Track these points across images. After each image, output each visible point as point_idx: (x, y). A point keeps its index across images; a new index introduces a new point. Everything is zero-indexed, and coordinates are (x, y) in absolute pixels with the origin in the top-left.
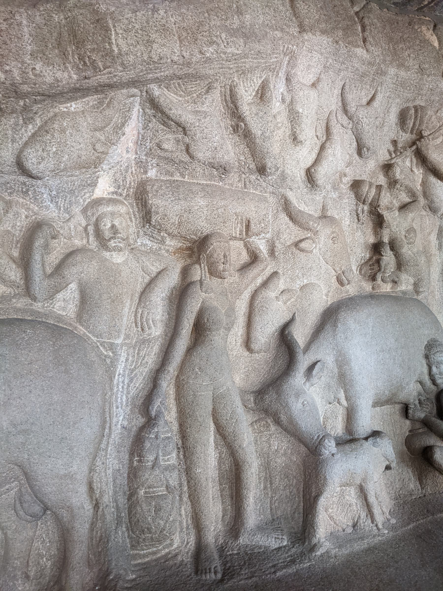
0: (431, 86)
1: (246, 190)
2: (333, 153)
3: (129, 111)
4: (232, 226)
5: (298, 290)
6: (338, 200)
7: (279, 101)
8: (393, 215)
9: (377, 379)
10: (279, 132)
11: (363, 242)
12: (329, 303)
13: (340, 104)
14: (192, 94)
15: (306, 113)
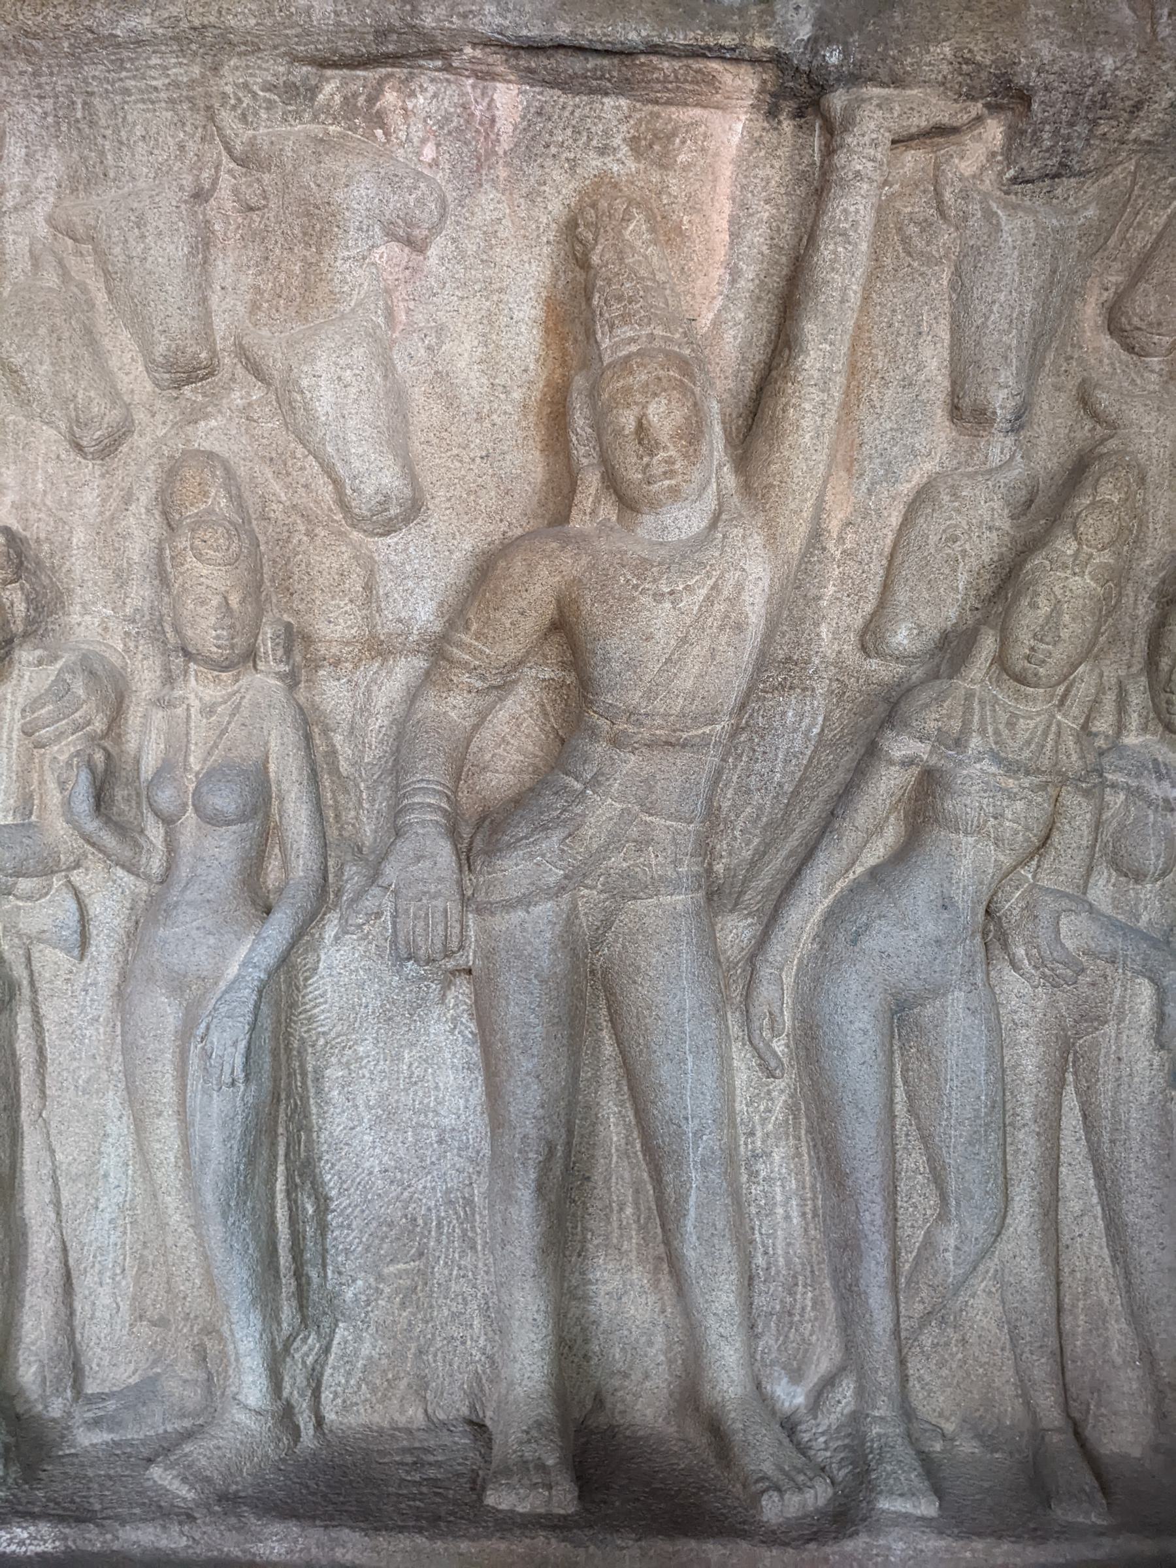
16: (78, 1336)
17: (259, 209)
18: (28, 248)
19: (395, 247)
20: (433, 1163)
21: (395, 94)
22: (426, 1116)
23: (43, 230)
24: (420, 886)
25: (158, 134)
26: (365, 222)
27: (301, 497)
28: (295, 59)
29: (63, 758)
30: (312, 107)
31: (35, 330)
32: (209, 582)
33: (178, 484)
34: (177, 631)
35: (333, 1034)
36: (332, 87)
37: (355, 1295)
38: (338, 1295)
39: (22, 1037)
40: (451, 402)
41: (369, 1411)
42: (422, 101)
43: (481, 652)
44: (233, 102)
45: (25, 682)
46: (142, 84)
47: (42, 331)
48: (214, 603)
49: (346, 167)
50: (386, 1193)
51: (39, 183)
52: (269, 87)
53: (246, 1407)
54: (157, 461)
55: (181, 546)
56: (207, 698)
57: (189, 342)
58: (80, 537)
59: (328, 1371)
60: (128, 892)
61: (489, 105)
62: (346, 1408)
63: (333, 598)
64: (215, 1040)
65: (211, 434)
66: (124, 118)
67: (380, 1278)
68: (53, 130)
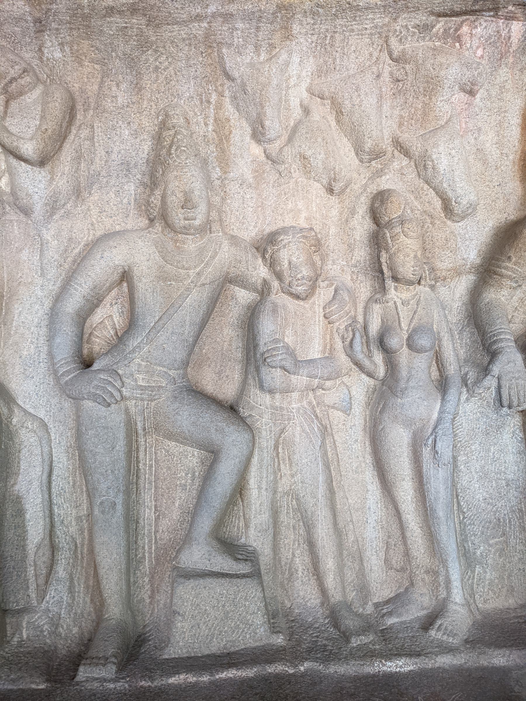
16: (368, 578)
17: (403, 80)
18: (299, 103)
19: (462, 94)
20: (505, 495)
21: (467, 27)
22: (500, 475)
23: (305, 95)
24: (511, 375)
25: (361, 49)
26: (452, 84)
27: (427, 207)
28: (432, 13)
29: (342, 327)
30: (430, 34)
31: (316, 139)
32: (411, 247)
33: (390, 204)
34: (391, 269)
35: (463, 441)
36: (440, 25)
37: (481, 553)
38: (475, 553)
39: (330, 450)
40: (485, 162)
41: (494, 602)
42: (479, 30)
43: (517, 270)
44: (398, 33)
45: (322, 295)
46: (360, 27)
47: (320, 140)
48: (412, 255)
49: (447, 60)
50: (486, 508)
51: (304, 74)
52: (417, 26)
53: (456, 603)
54: (365, 195)
55: (396, 231)
56: (403, 298)
57: (380, 141)
58: (333, 230)
59: (475, 586)
60: (366, 385)
61: (509, 31)
62: (485, 602)
63: (443, 251)
64: (440, 446)
65: (386, 182)
66: (347, 43)
67: (490, 545)
68: (313, 49)
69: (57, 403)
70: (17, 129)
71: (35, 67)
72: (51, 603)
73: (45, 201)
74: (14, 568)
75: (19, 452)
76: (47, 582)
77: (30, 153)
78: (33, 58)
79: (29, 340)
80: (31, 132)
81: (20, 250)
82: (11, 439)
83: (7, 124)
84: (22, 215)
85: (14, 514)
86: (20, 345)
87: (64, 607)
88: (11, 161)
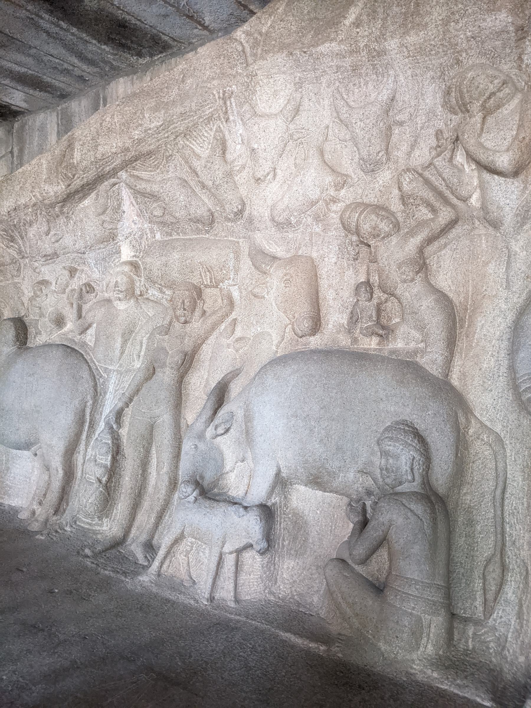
0: (469, 34)
1: (225, 238)
2: (301, 181)
3: (118, 194)
4: (201, 275)
5: (252, 338)
6: (322, 233)
7: (239, 144)
8: (387, 244)
9: (286, 448)
10: (243, 174)
11: (353, 283)
12: (278, 355)
13: (335, 114)
14: (159, 166)
15: (263, 147)
69: (516, 419)
70: (493, 144)
71: (513, 77)
72: (498, 622)
73: (516, 211)
74: (463, 575)
75: (473, 462)
76: (495, 599)
77: (506, 165)
78: (511, 69)
79: (490, 353)
80: (506, 143)
81: (486, 264)
82: (466, 449)
83: (483, 140)
84: (491, 228)
85: (466, 522)
86: (480, 357)
87: (511, 630)
88: (484, 176)
